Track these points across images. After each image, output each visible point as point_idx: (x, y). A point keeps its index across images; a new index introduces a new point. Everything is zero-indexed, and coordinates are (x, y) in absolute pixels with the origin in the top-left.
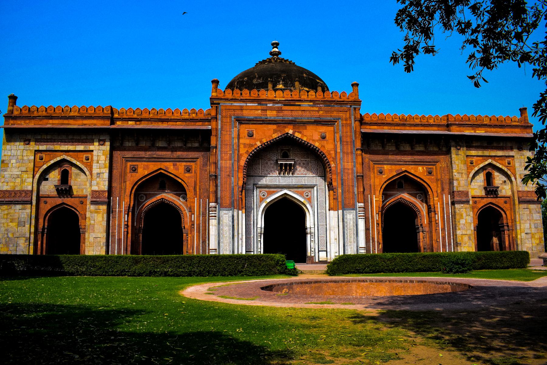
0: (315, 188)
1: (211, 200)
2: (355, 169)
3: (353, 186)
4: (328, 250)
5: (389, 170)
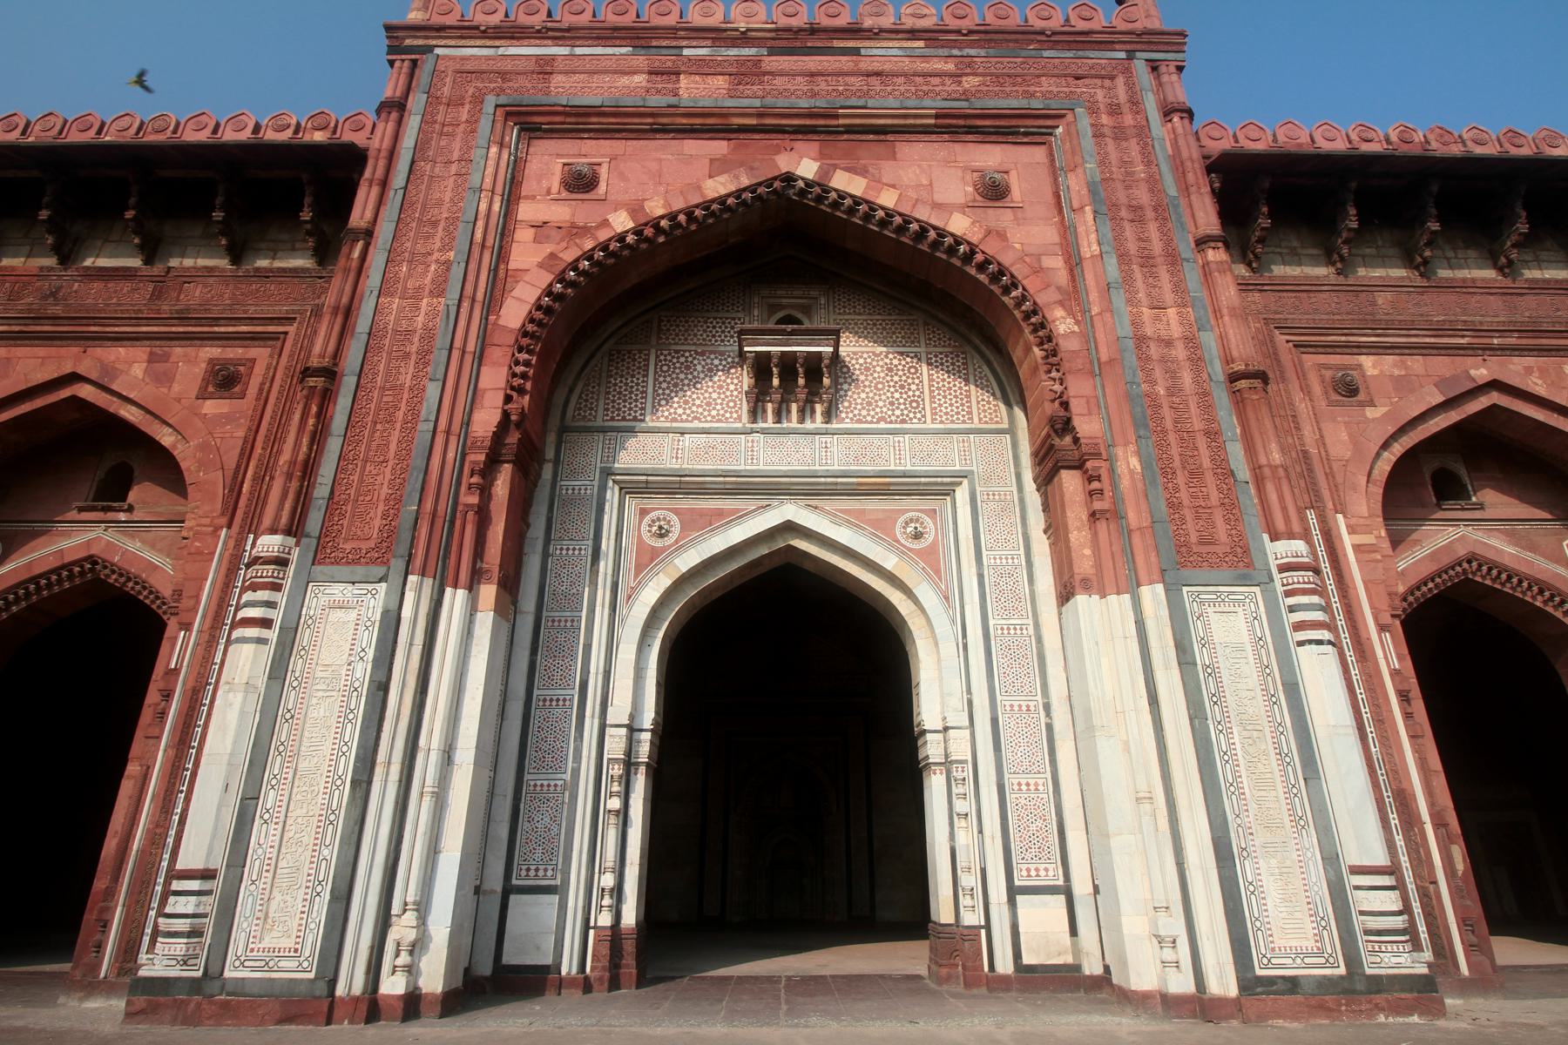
0: (962, 494)
1: (267, 521)
2: (1209, 340)
3: (1213, 434)
4: (1082, 887)
5: (1397, 380)
